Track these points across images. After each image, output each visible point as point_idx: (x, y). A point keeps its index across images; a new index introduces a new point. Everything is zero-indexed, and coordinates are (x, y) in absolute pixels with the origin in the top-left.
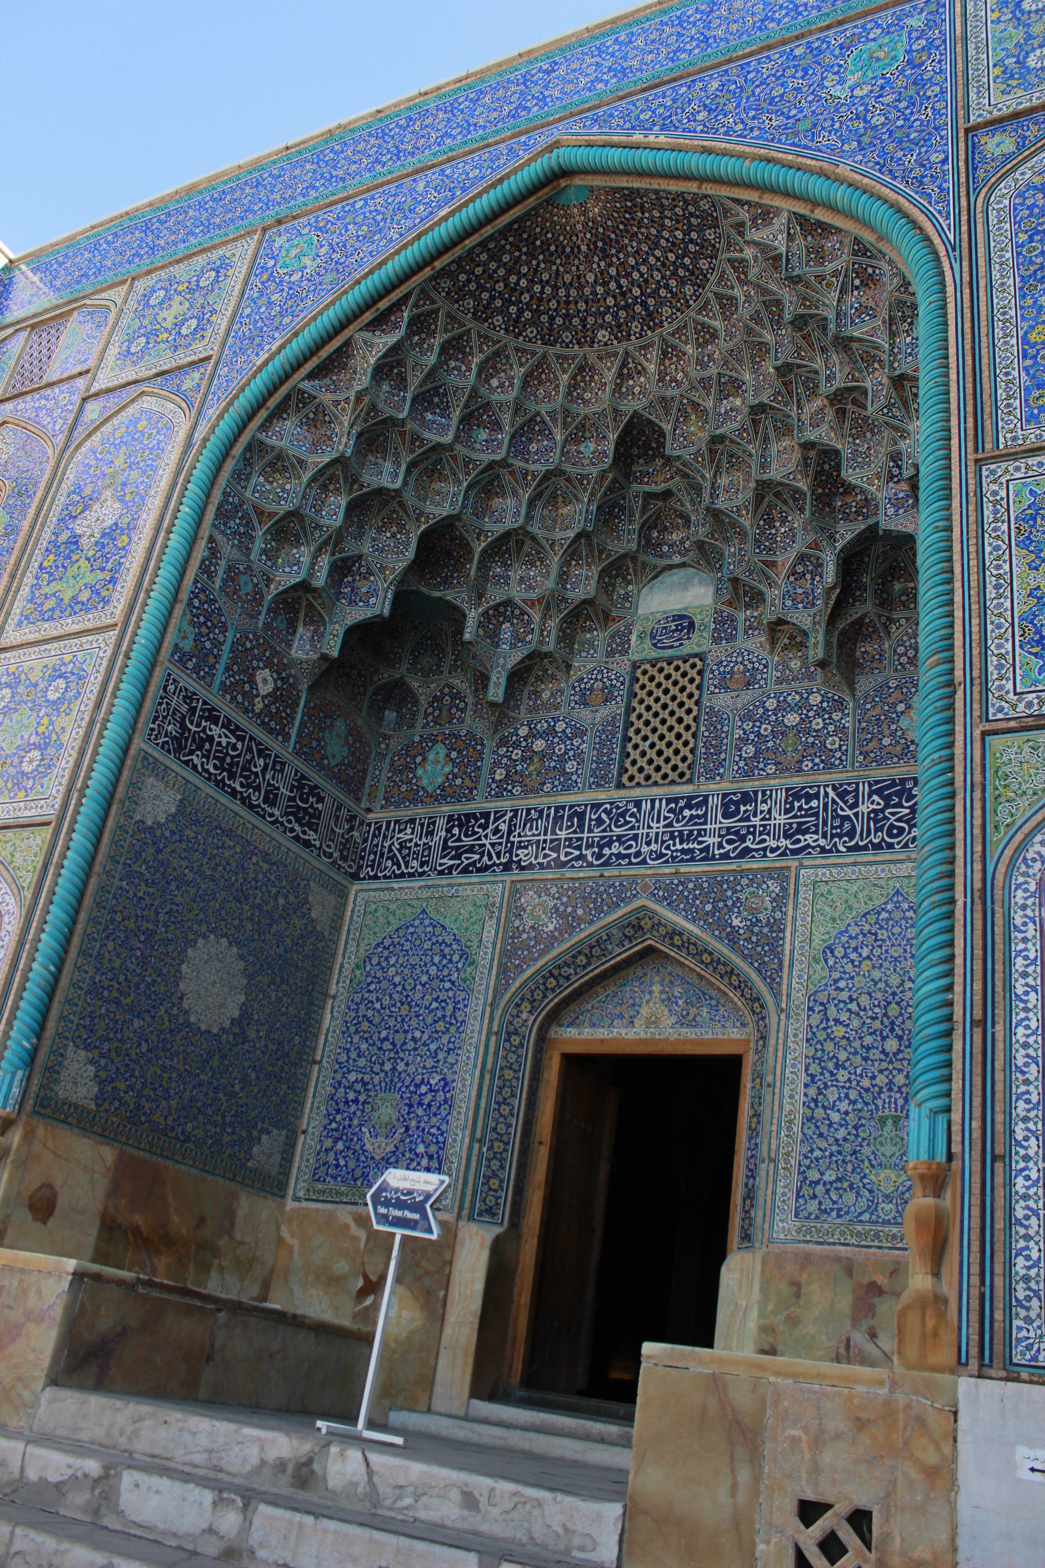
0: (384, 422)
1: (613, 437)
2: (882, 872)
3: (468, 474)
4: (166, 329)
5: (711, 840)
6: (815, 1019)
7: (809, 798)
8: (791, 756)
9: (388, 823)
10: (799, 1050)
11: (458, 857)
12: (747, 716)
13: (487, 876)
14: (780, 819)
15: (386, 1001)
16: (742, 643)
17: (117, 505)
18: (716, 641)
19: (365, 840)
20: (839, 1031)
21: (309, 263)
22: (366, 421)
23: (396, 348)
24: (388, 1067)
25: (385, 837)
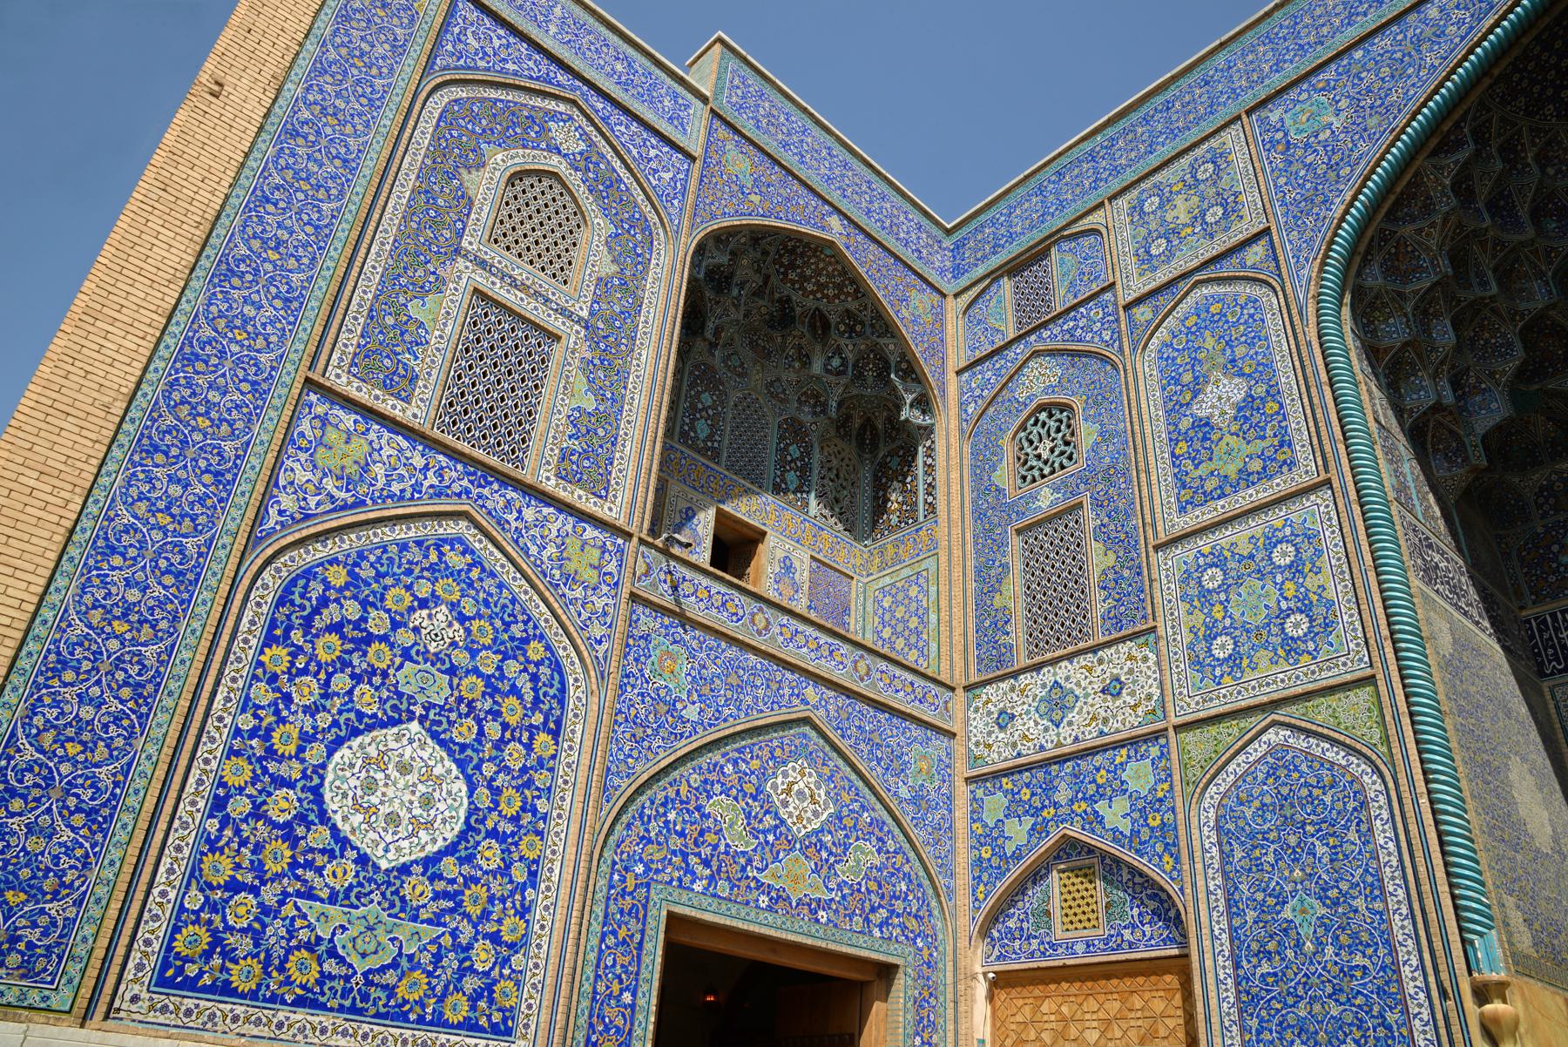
0: (1467, 236)
3: (1551, 263)
4: (1185, 225)
9: (1553, 616)
17: (1237, 380)
19: (1532, 637)
21: (1333, 119)
22: (1453, 239)
23: (1467, 164)
25: (1557, 630)
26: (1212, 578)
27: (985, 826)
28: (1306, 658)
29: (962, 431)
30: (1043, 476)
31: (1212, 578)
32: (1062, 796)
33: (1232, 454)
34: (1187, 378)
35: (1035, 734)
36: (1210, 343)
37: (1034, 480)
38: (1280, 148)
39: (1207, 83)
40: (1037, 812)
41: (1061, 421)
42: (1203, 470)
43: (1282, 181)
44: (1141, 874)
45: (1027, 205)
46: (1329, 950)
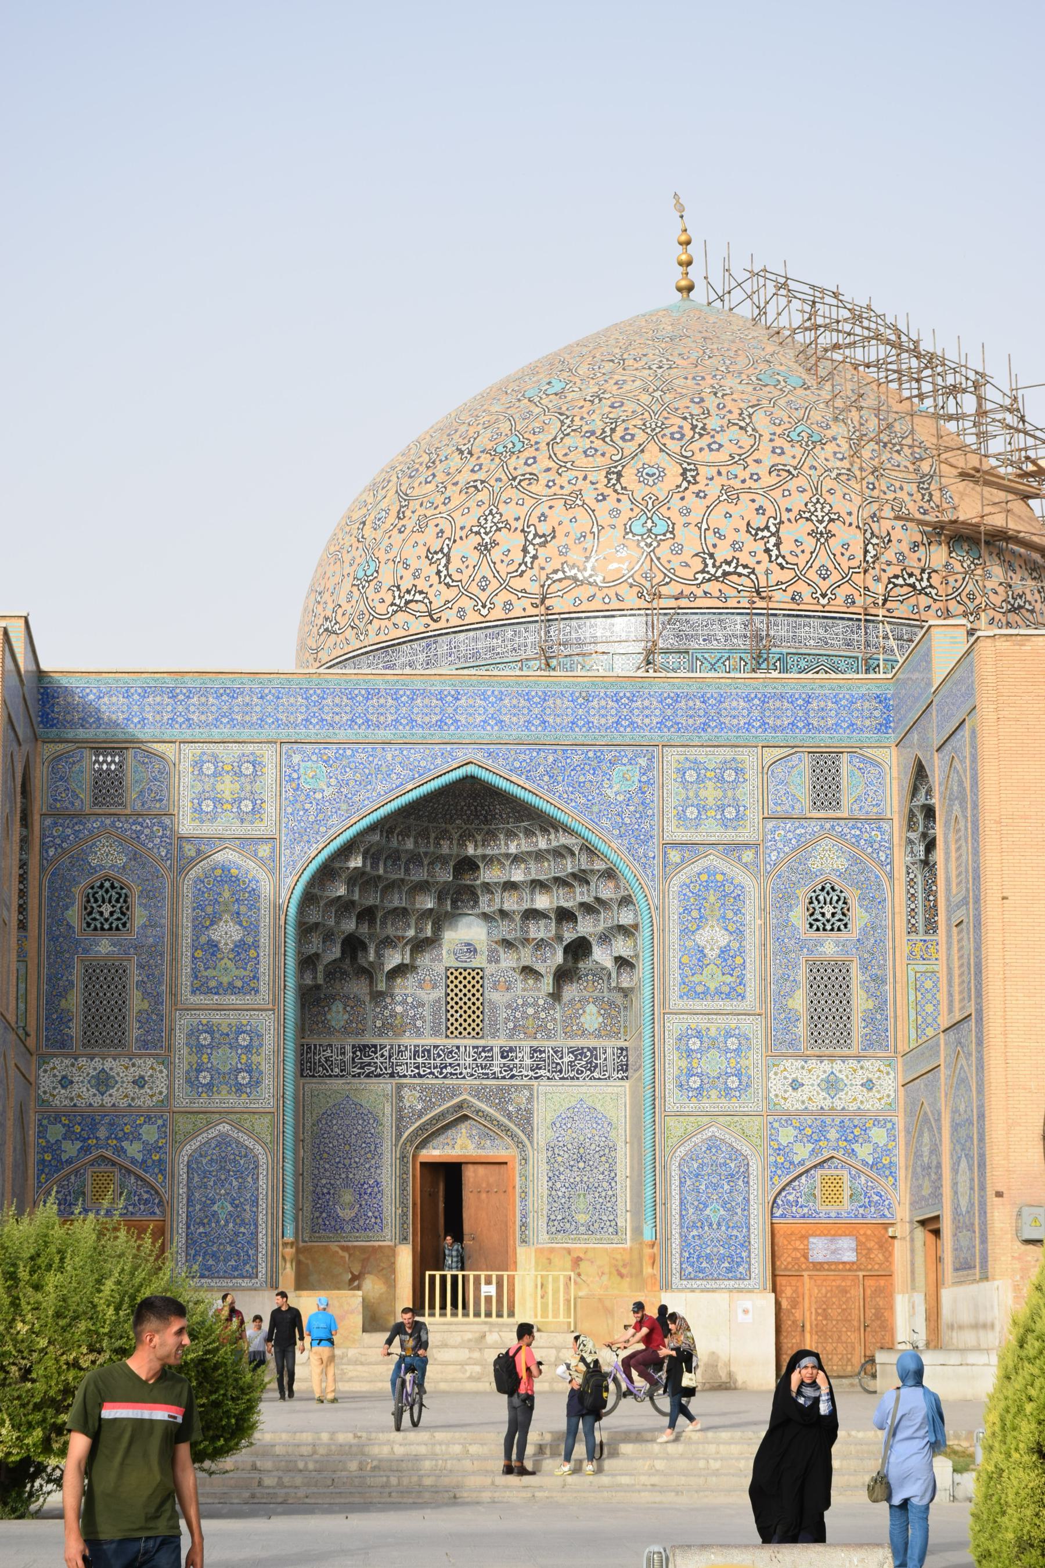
1: (452, 864)
2: (575, 1090)
5: (496, 1069)
6: (550, 1154)
7: (541, 1052)
8: (531, 1031)
10: (544, 1167)
11: (362, 1068)
12: (508, 1006)
13: (380, 1080)
14: (528, 1062)
15: (335, 1143)
16: (504, 964)
18: (490, 962)
20: (560, 1159)
24: (343, 1176)
26: (205, 1039)
27: (48, 1142)
28: (244, 1096)
29: (42, 869)
30: (102, 929)
31: (205, 1039)
32: (102, 1133)
33: (227, 971)
34: (209, 910)
35: (84, 1093)
36: (226, 894)
37: (95, 929)
38: (294, 785)
39: (262, 697)
40: (85, 1140)
41: (120, 895)
42: (210, 973)
43: (289, 810)
44: (142, 1180)
45: (114, 699)
46: (231, 1225)
